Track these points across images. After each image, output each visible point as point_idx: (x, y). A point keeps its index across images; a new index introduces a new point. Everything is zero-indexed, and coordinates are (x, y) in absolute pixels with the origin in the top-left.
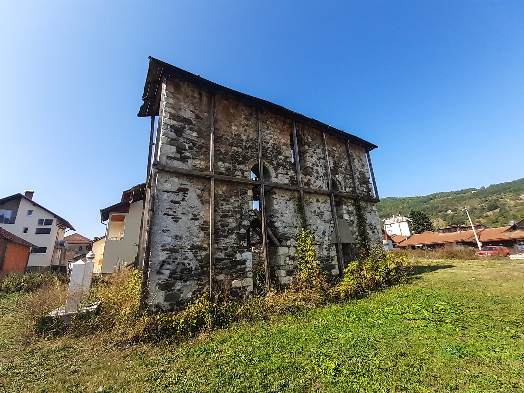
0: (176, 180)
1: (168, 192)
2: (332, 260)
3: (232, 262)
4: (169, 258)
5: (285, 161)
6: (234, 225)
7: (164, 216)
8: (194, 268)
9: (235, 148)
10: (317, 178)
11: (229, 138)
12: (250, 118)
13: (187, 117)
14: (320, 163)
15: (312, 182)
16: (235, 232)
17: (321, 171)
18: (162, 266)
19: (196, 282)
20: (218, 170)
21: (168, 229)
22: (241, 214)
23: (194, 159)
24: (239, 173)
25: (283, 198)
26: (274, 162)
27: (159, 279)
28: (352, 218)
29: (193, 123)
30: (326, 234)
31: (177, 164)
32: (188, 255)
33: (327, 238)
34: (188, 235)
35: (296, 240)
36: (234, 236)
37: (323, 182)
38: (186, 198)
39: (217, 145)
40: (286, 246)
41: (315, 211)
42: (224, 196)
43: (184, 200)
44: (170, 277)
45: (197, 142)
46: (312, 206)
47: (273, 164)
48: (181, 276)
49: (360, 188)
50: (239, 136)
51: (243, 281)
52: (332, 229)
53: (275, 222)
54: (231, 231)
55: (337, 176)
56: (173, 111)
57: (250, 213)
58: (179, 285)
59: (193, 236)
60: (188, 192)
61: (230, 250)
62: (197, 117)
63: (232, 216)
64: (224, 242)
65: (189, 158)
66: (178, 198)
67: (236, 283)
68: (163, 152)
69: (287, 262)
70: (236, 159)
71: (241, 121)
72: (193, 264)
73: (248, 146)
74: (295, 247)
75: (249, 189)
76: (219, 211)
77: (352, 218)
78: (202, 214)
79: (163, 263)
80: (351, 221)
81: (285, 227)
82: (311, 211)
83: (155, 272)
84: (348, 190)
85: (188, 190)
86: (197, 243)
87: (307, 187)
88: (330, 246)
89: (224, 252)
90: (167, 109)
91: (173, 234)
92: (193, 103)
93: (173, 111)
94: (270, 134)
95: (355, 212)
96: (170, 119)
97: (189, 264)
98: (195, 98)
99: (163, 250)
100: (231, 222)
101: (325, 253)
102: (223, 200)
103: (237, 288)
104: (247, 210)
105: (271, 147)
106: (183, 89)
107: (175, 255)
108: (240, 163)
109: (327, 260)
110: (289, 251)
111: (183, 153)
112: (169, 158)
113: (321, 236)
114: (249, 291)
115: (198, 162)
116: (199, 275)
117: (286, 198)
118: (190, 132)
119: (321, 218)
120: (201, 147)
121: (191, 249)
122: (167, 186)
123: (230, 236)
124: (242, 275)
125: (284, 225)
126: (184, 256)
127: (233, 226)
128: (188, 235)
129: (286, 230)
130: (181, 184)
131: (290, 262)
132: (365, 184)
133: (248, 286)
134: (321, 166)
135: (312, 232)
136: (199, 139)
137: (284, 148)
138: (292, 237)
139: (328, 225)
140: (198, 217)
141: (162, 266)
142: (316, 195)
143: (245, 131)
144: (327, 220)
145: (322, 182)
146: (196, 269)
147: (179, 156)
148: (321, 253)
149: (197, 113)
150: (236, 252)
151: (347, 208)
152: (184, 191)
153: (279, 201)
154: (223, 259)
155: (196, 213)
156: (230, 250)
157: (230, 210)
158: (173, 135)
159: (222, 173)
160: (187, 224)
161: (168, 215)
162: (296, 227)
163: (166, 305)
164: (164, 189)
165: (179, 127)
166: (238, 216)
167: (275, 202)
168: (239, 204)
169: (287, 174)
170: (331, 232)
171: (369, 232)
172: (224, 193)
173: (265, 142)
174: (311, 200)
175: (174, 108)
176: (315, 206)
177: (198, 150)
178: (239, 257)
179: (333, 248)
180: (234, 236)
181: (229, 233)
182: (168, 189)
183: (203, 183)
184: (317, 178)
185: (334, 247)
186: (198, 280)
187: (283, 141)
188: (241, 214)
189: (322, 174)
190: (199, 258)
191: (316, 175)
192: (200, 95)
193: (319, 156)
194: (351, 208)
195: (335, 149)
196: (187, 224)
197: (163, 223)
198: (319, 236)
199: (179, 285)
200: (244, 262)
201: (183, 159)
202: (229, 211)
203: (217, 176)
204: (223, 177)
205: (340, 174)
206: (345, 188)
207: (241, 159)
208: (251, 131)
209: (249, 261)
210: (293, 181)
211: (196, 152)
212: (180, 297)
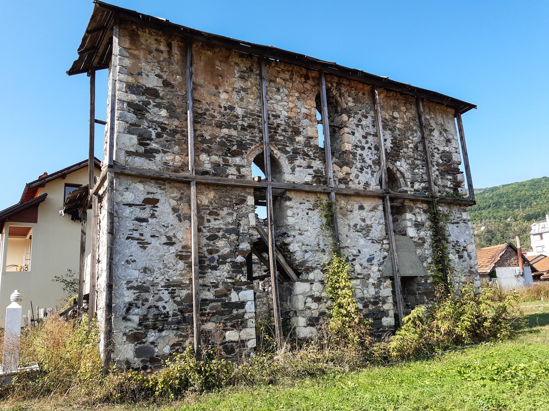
0: (140, 186)
1: (130, 205)
2: (384, 302)
3: (225, 305)
4: (137, 299)
5: (307, 144)
7: (127, 241)
8: (171, 313)
9: (225, 131)
10: (362, 169)
11: (216, 114)
12: (249, 77)
13: (150, 86)
14: (367, 142)
15: (352, 177)
16: (229, 260)
17: (369, 156)
18: (128, 310)
19: (175, 332)
20: (201, 168)
21: (133, 258)
22: (238, 234)
23: (165, 152)
24: (232, 171)
25: (302, 206)
26: (288, 149)
27: (125, 327)
28: (422, 234)
29: (161, 95)
30: (375, 261)
31: (140, 163)
32: (162, 296)
33: (375, 268)
34: (161, 266)
35: (324, 271)
36: (227, 267)
37: (372, 175)
38: (156, 213)
39: (198, 126)
40: (307, 281)
41: (355, 226)
42: (211, 208)
43: (153, 216)
44: (140, 324)
45: (168, 125)
46: (350, 216)
47: (286, 152)
48: (155, 325)
49: (440, 182)
50: (232, 108)
51: (242, 332)
52: (386, 253)
53: (288, 244)
54: (223, 260)
55: (398, 163)
56: (130, 79)
57: (251, 231)
58: (152, 336)
59: (169, 268)
60: (158, 205)
61: (221, 287)
62: (166, 84)
63: (224, 236)
64: (212, 277)
65: (157, 151)
66: (145, 214)
67: (231, 335)
68: (120, 146)
69: (307, 305)
71: (233, 83)
72: (171, 308)
73: (246, 125)
74: (322, 282)
75: (249, 194)
76: (204, 230)
77: (422, 234)
78: (179, 235)
79: (130, 307)
80: (420, 239)
81: (306, 252)
82: (349, 225)
83: (121, 318)
84: (417, 186)
85: (157, 201)
86: (175, 278)
87: (343, 186)
88: (380, 281)
89: (213, 290)
90: (122, 76)
91: (141, 264)
92: (159, 62)
93: (130, 79)
94: (282, 100)
95: (428, 224)
96: (126, 92)
97: (164, 308)
98: (162, 52)
99: (128, 289)
100: (223, 246)
101: (372, 291)
102: (211, 214)
103: (232, 342)
104: (246, 227)
105: (283, 122)
106: (142, 40)
107: (145, 295)
108: (235, 154)
109: (375, 303)
110: (311, 289)
111: (148, 144)
112: (129, 153)
113: (366, 264)
114: (250, 346)
115: (171, 157)
116: (179, 323)
117: (308, 205)
118: (157, 109)
119: (366, 236)
120: (175, 132)
121: (167, 286)
122: (129, 197)
123: (221, 267)
124: (239, 323)
125: (304, 248)
126: (157, 297)
127: (226, 252)
128: (161, 266)
129: (307, 256)
130: (148, 193)
131: (314, 306)
132: (449, 174)
133: (249, 340)
134: (370, 148)
135: (350, 258)
136: (171, 120)
137: (305, 122)
138: (316, 268)
139: (379, 246)
140: (174, 240)
141: (128, 310)
142: (358, 199)
143: (242, 99)
144: (376, 239)
145: (370, 175)
146: (175, 315)
147: (142, 149)
148: (365, 292)
149: (165, 77)
150: (229, 290)
151: (413, 219)
152: (152, 202)
153: (295, 210)
154: (212, 301)
155: (171, 234)
156: (221, 287)
157: (220, 229)
158: (132, 117)
159: (206, 173)
160: (159, 251)
161: (133, 239)
162: (323, 251)
163: (137, 362)
164: (125, 201)
165: (141, 103)
166: (233, 237)
167: (289, 212)
168: (234, 218)
169: (310, 167)
170: (384, 258)
171: (453, 256)
172: (211, 203)
173: (273, 115)
174: (349, 207)
175: (132, 75)
176: (356, 217)
177: (169, 138)
178: (234, 297)
179: (385, 284)
180: (227, 267)
181: (219, 263)
182: (130, 201)
183: (179, 189)
184: (362, 169)
185: (388, 282)
186: (178, 329)
187: (304, 110)
188: (238, 234)
189: (370, 162)
190: (178, 299)
191: (359, 165)
192: (169, 46)
193: (367, 130)
194: (422, 218)
195: (396, 115)
196: (159, 251)
197: (127, 251)
198: (361, 265)
199: (152, 336)
200: (241, 305)
201: (149, 154)
202: (219, 230)
203: (200, 178)
204: (209, 179)
205: (403, 160)
206: (412, 183)
207: (235, 148)
208: (251, 98)
209: (249, 303)
210: (320, 178)
211: (167, 141)
212: (154, 352)
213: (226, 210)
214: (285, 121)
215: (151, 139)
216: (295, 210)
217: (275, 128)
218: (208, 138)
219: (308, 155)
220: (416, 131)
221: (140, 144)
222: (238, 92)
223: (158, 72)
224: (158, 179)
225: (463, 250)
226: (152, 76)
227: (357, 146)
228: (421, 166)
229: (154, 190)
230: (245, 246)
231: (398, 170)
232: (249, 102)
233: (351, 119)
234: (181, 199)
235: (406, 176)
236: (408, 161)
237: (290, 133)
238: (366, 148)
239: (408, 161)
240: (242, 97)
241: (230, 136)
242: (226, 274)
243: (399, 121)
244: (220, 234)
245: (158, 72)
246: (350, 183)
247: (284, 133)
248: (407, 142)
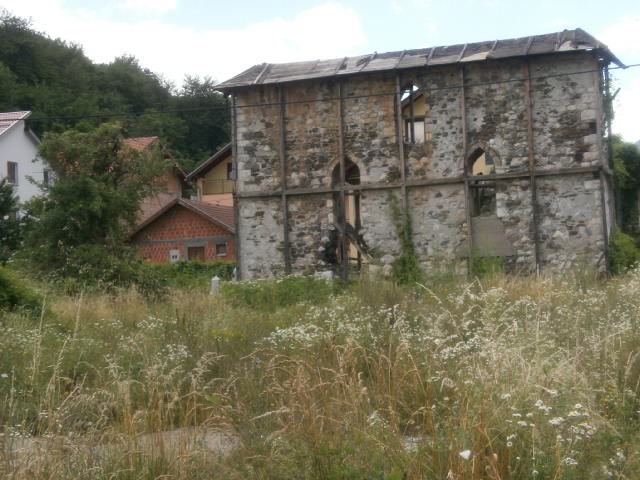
0: (253, 205)
1: (248, 218)
5: (384, 144)
6: (311, 243)
9: (311, 150)
13: (257, 130)
14: (451, 128)
20: (291, 185)
22: (320, 230)
23: (268, 177)
24: (316, 182)
26: (364, 153)
28: (516, 212)
31: (254, 189)
33: (450, 251)
36: (311, 255)
37: (455, 161)
39: (289, 152)
41: (431, 213)
50: (315, 130)
52: (464, 236)
54: (308, 250)
55: (491, 141)
62: (268, 125)
63: (309, 234)
64: (300, 262)
70: (313, 164)
73: (327, 140)
75: (327, 198)
77: (516, 212)
80: (513, 218)
81: (378, 240)
84: (515, 162)
89: (302, 271)
91: (255, 255)
94: (358, 111)
100: (308, 240)
101: (443, 270)
102: (299, 217)
105: (360, 130)
107: (258, 274)
112: (246, 183)
120: (274, 161)
125: (376, 237)
129: (380, 243)
132: (568, 138)
135: (422, 243)
137: (382, 124)
138: (386, 253)
139: (457, 230)
143: (324, 121)
147: (253, 178)
149: (267, 120)
152: (260, 214)
153: (368, 206)
155: (272, 234)
159: (295, 187)
166: (316, 233)
170: (462, 240)
173: (352, 126)
174: (424, 197)
180: (311, 255)
183: (277, 202)
187: (381, 113)
188: (320, 230)
193: (454, 114)
201: (258, 181)
202: (305, 229)
206: (509, 161)
207: (317, 163)
210: (394, 174)
213: (310, 213)
215: (258, 170)
216: (368, 206)
218: (297, 158)
219: (383, 155)
220: (523, 98)
221: (253, 175)
222: (322, 114)
223: (262, 118)
224: (264, 197)
225: (578, 226)
226: (258, 122)
227: (439, 134)
228: (525, 138)
229: (260, 206)
230: (325, 239)
231: (490, 148)
232: (330, 121)
234: (278, 210)
235: (501, 152)
236: (506, 136)
237: (367, 138)
239: (506, 136)
241: (314, 154)
242: (310, 260)
243: (499, 92)
244: (306, 232)
245: (262, 118)
246: (427, 173)
248: (506, 115)
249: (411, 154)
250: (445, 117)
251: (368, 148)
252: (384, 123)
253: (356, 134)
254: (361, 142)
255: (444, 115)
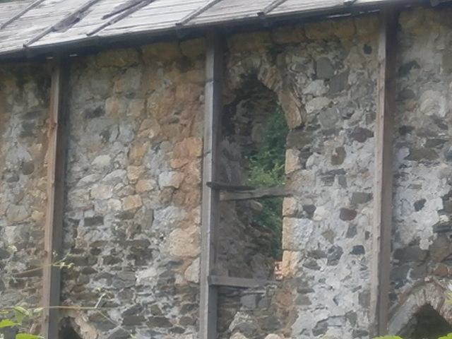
5: (167, 286)
105: (107, 236)
187: (167, 179)
214: (114, 232)
217: (86, 260)
227: (317, 254)
233: (310, 161)
237: (125, 263)
238: (346, 252)
240: (22, 191)
247: (106, 269)
249: (240, 318)
250: (337, 196)
251: (126, 295)
252: (168, 215)
253: (96, 251)
254: (109, 277)
255: (334, 190)
